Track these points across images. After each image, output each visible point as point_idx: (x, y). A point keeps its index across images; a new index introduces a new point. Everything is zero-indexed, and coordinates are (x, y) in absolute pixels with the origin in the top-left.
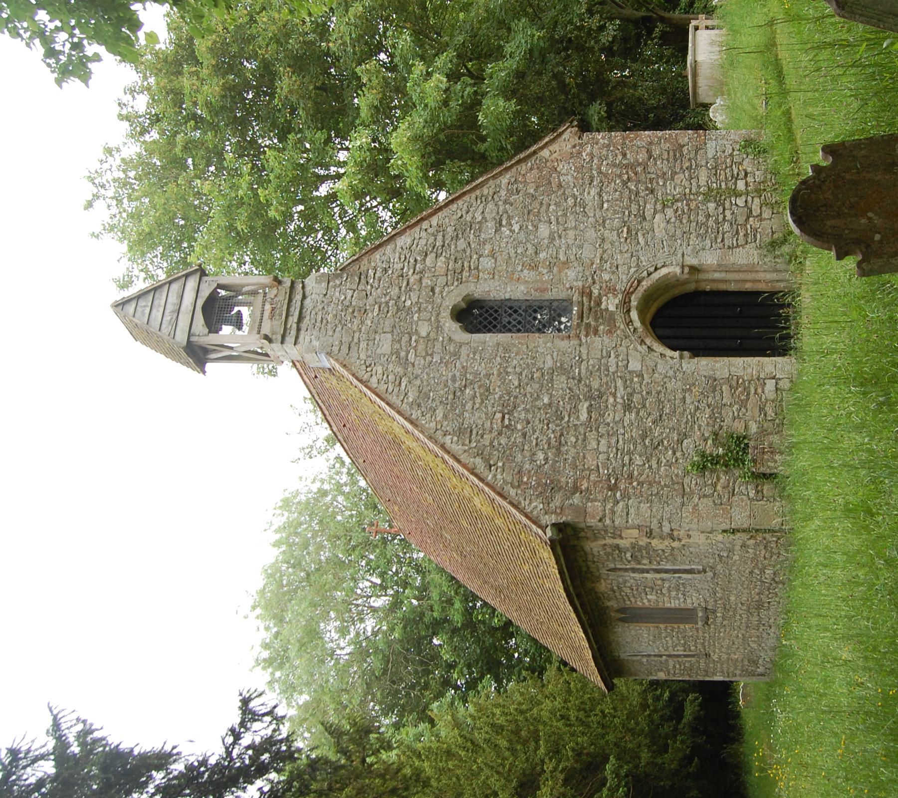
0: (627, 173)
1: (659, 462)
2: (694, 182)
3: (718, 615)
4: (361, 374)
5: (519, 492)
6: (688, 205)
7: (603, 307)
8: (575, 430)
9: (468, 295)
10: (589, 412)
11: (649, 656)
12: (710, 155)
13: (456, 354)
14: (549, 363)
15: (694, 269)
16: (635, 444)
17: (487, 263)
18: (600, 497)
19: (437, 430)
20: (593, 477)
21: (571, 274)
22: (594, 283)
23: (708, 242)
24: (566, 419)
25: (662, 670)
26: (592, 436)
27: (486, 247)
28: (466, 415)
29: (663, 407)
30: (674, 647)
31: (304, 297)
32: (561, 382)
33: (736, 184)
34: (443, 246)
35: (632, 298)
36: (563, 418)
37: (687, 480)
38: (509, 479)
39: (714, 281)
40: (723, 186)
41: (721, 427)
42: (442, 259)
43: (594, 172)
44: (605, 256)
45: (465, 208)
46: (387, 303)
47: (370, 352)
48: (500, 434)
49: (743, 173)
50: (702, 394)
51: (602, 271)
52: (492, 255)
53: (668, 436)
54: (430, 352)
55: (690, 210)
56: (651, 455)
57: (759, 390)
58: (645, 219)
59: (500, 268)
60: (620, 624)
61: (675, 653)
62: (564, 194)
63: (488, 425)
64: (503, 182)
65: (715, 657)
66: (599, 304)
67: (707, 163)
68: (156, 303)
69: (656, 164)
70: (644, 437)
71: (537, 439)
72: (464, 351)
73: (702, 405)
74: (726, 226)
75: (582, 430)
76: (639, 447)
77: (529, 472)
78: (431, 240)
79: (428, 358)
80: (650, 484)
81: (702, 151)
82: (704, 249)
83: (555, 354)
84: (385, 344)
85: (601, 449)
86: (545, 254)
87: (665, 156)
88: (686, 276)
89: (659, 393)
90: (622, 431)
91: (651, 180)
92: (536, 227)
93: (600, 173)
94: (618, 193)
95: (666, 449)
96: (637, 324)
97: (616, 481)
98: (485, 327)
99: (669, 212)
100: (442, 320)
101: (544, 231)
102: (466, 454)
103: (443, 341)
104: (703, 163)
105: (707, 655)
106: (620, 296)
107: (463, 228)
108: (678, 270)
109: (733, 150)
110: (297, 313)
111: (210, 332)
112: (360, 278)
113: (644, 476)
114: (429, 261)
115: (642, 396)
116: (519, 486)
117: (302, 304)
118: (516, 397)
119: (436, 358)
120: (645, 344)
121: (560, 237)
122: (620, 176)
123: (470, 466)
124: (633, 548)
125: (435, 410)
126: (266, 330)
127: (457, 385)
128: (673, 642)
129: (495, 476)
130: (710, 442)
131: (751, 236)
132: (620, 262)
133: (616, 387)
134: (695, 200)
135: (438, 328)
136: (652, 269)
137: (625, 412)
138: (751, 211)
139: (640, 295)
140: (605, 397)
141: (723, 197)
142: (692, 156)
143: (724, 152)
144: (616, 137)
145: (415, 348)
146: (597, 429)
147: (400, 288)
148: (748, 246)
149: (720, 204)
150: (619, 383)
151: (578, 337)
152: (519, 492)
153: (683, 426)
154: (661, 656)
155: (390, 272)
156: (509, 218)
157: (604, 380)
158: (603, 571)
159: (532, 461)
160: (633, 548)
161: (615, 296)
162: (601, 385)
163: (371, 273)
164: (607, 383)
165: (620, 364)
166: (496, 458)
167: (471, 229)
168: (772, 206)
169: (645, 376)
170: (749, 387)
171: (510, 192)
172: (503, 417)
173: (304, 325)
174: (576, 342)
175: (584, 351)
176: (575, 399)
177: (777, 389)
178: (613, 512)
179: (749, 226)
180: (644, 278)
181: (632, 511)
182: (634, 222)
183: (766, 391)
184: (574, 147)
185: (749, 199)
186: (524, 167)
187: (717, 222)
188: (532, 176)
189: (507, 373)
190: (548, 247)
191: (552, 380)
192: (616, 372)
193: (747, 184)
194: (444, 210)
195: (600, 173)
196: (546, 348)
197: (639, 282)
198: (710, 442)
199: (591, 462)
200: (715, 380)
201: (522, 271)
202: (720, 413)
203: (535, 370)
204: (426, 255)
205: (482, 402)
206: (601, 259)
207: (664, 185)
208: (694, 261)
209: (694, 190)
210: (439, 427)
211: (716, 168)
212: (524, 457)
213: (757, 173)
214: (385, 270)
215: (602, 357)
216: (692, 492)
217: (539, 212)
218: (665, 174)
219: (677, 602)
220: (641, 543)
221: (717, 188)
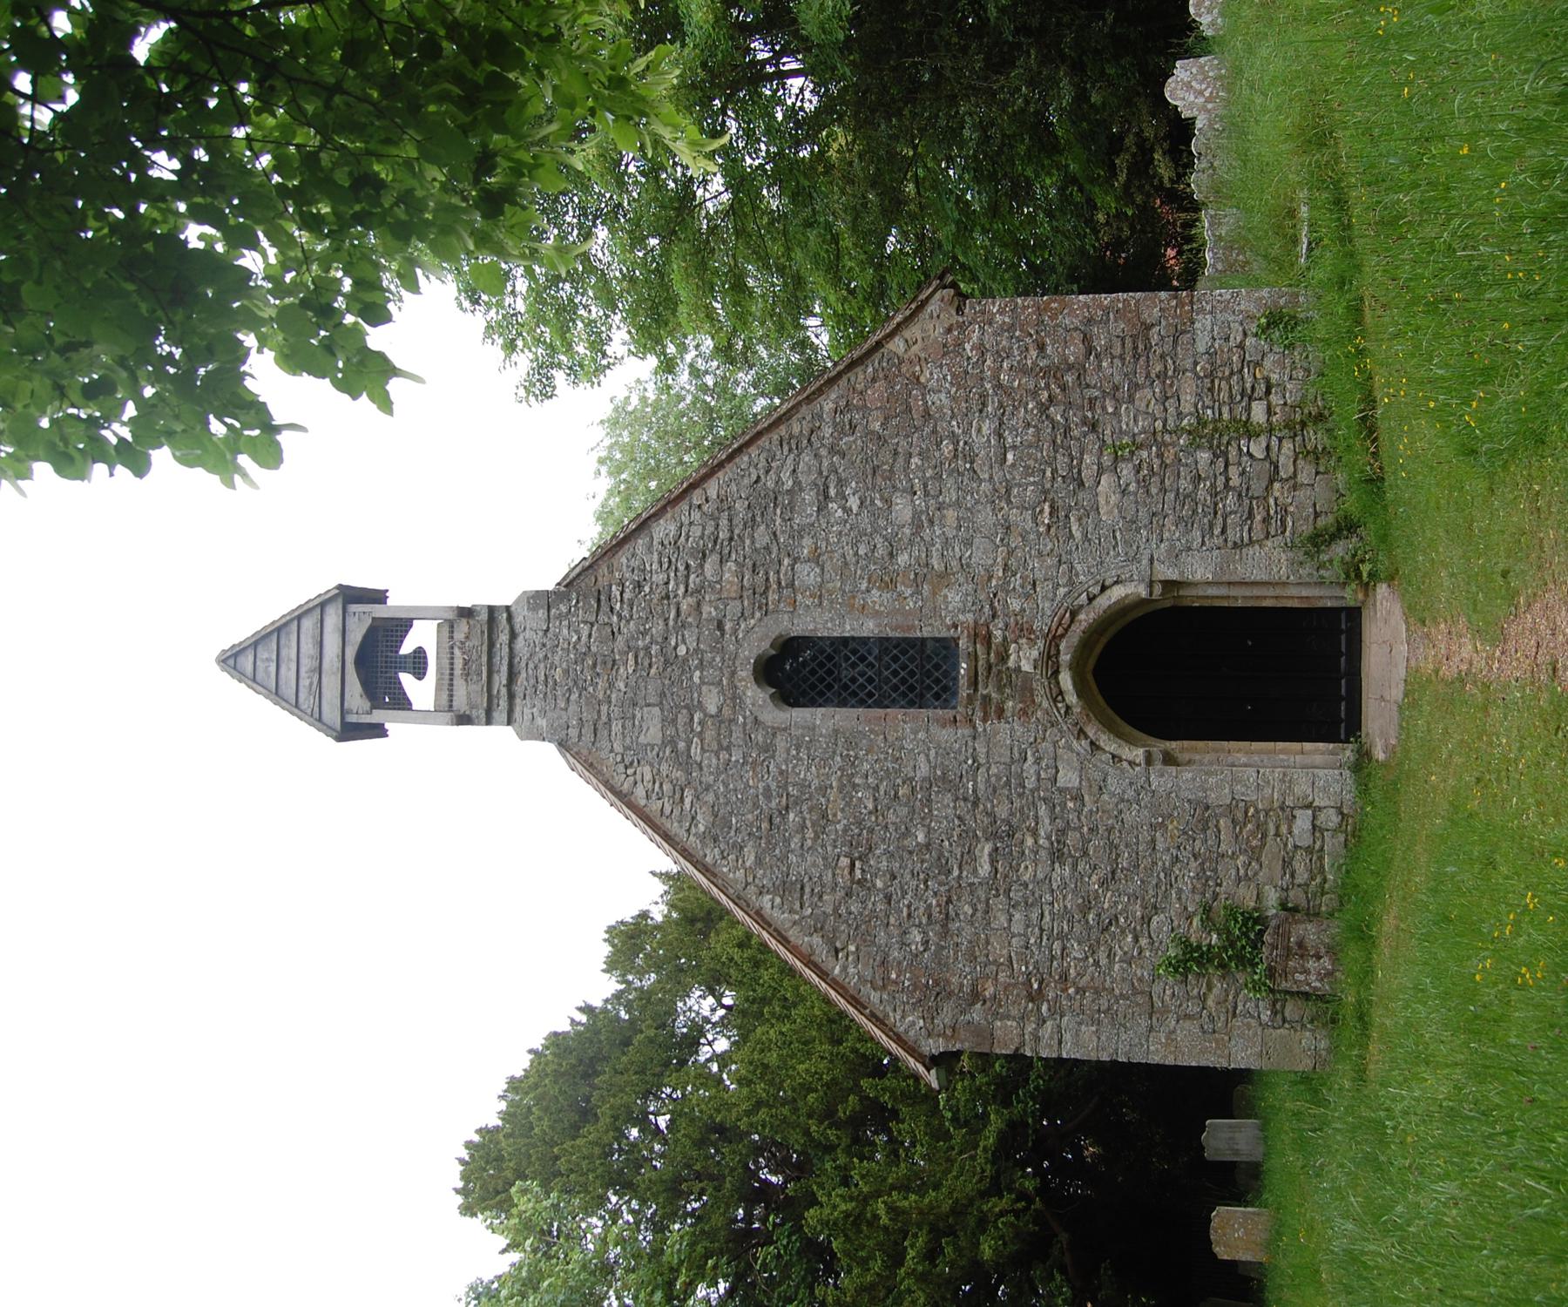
0: (1048, 386)
2: (1171, 405)
6: (1160, 455)
7: (1011, 663)
8: (972, 894)
13: (768, 749)
14: (924, 770)
15: (1168, 585)
17: (807, 575)
18: (1014, 1012)
19: (747, 884)
20: (1002, 977)
21: (954, 597)
22: (994, 616)
24: (956, 873)
26: (999, 904)
28: (793, 858)
29: (1118, 855)
31: (513, 635)
32: (944, 805)
33: (1248, 409)
34: (731, 539)
35: (1062, 646)
37: (1157, 989)
38: (868, 974)
40: (1226, 416)
41: (1216, 896)
43: (988, 386)
45: (763, 463)
46: (647, 649)
47: (628, 740)
48: (849, 895)
50: (1185, 833)
51: (1008, 592)
52: (815, 558)
53: (1125, 910)
54: (725, 744)
57: (1284, 829)
58: (1081, 484)
59: (830, 585)
62: (934, 432)
63: (828, 877)
64: (826, 408)
66: (1003, 658)
67: (1196, 363)
68: (284, 652)
69: (1100, 366)
70: (1085, 908)
71: (909, 907)
72: (781, 743)
74: (1231, 499)
75: (981, 893)
76: (1077, 928)
77: (899, 963)
78: (709, 529)
79: (724, 755)
80: (1097, 992)
81: (1185, 338)
82: (1189, 549)
83: (932, 752)
84: (652, 732)
85: (1015, 929)
86: (906, 557)
87: (1117, 351)
90: (1048, 897)
92: (888, 502)
93: (999, 386)
94: (1031, 430)
95: (1123, 932)
96: (1072, 698)
97: (1040, 984)
99: (1126, 470)
101: (903, 509)
102: (797, 928)
103: (745, 724)
104: (1188, 364)
106: (1040, 643)
109: (1245, 334)
110: (505, 668)
111: (374, 707)
112: (599, 601)
113: (1087, 978)
114: (709, 567)
115: (1082, 835)
117: (511, 649)
119: (736, 756)
120: (1086, 737)
121: (931, 522)
122: (1034, 394)
123: (805, 949)
125: (742, 848)
126: (460, 703)
127: (773, 805)
129: (844, 969)
130: (1196, 921)
131: (1276, 522)
132: (1039, 575)
133: (1036, 817)
134: (1173, 444)
135: (736, 699)
136: (1096, 590)
138: (1276, 467)
141: (1225, 439)
142: (1167, 348)
143: (1227, 339)
144: (1025, 308)
145: (700, 735)
147: (666, 620)
148: (1269, 543)
149: (1219, 453)
150: (1043, 810)
155: (647, 589)
156: (841, 483)
157: (1017, 804)
159: (903, 944)
162: (1012, 814)
163: (615, 590)
164: (1021, 810)
165: (1043, 775)
166: (844, 936)
167: (776, 506)
168: (1315, 455)
169: (1086, 798)
170: (1266, 823)
171: (840, 431)
172: (853, 865)
173: (518, 689)
174: (967, 731)
175: (982, 750)
176: (969, 838)
177: (1314, 826)
178: (1037, 1039)
179: (1272, 501)
181: (1067, 1037)
182: (1062, 491)
183: (1296, 831)
184: (949, 330)
185: (1274, 442)
188: (876, 393)
189: (854, 786)
191: (929, 800)
192: (1038, 789)
193: (1270, 411)
194: (728, 467)
195: (999, 386)
196: (916, 737)
197: (1074, 614)
198: (1196, 921)
199: (998, 950)
200: (1207, 808)
202: (1215, 870)
203: (899, 781)
204: (704, 555)
205: (817, 837)
206: (1006, 568)
207: (1116, 413)
208: (1172, 575)
209: (1171, 424)
210: (750, 879)
211: (1211, 375)
212: (890, 936)
214: (639, 586)
215: (1013, 761)
216: (1166, 1010)
217: (891, 471)
218: (1116, 388)
221: (1215, 421)
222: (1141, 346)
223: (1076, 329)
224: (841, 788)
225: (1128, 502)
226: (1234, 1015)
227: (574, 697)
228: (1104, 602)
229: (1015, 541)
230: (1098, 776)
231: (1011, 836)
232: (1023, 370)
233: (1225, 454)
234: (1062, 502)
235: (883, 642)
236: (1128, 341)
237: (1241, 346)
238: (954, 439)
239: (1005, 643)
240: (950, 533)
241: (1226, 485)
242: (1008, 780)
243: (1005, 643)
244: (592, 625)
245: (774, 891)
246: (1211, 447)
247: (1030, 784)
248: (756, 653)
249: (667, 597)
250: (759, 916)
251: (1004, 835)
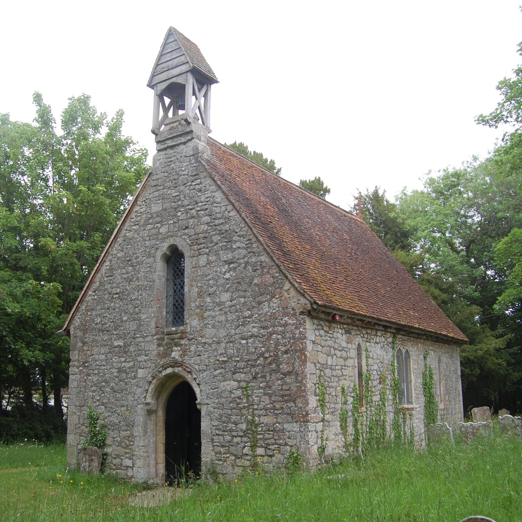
0: (270, 356)
1: (94, 391)
2: (263, 412)
4: (141, 199)
5: (84, 311)
6: (244, 407)
7: (175, 348)
10: (119, 346)
12: (286, 426)
13: (149, 256)
14: (143, 317)
16: (102, 376)
17: (203, 260)
19: (112, 255)
23: (216, 423)
24: (115, 333)
27: (214, 257)
31: (184, 143)
32: (132, 326)
33: (261, 447)
34: (215, 226)
35: (180, 368)
36: (115, 330)
37: (86, 408)
38: (89, 304)
40: (259, 436)
43: (271, 329)
44: (207, 346)
45: (242, 233)
48: (110, 294)
49: (271, 453)
51: (197, 345)
52: (209, 263)
53: (105, 396)
55: (241, 409)
56: (97, 387)
57: (127, 455)
59: (199, 271)
62: (254, 307)
66: (176, 345)
67: (279, 423)
68: (174, 52)
69: (278, 380)
70: (106, 381)
71: (106, 316)
72: (151, 260)
73: (120, 418)
74: (228, 438)
78: (218, 216)
79: (147, 238)
81: (290, 419)
82: (211, 420)
83: (148, 320)
87: (285, 387)
89: (126, 390)
91: (264, 377)
92: (227, 291)
93: (271, 334)
94: (253, 350)
96: (164, 373)
97: (87, 366)
99: (239, 393)
100: (168, 240)
101: (225, 297)
103: (156, 244)
104: (279, 420)
106: (180, 359)
107: (228, 237)
109: (291, 446)
110: (173, 144)
114: (207, 219)
115: (125, 379)
118: (126, 299)
121: (221, 310)
122: (268, 351)
123: (95, 280)
125: (122, 251)
129: (90, 295)
134: (248, 413)
135: (163, 240)
137: (117, 369)
139: (182, 374)
142: (286, 410)
143: (289, 438)
146: (110, 352)
147: (189, 205)
148: (213, 454)
150: (131, 364)
152: (84, 311)
153: (110, 405)
155: (199, 194)
157: (133, 354)
161: (181, 356)
162: (131, 352)
164: (132, 356)
165: (141, 363)
167: (227, 242)
169: (135, 380)
171: (254, 265)
172: (117, 294)
175: (148, 339)
178: (73, 366)
179: (228, 455)
180: (192, 375)
183: (127, 460)
184: (293, 309)
186: (274, 271)
187: (231, 431)
188: (268, 279)
189: (138, 291)
190: (214, 302)
191: (135, 320)
192: (137, 362)
197: (190, 372)
199: (96, 350)
200: (133, 426)
201: (197, 287)
204: (210, 215)
205: (125, 279)
207: (260, 388)
209: (256, 412)
210: (113, 256)
211: (274, 430)
213: (271, 465)
214: (200, 191)
215: (145, 351)
217: (239, 290)
221: (257, 432)
222: (286, 398)
223: (294, 368)
224: (138, 286)
225: (227, 394)
226: (80, 436)
227: (166, 174)
229: (214, 346)
230: (141, 384)
231: (125, 352)
232: (277, 344)
233: (245, 436)
234: (226, 366)
235: (183, 295)
236: (289, 392)
237: (286, 444)
238: (250, 316)
239: (180, 345)
240: (216, 318)
241: (233, 436)
243: (180, 345)
244: (188, 175)
245: (111, 266)
246: (248, 430)
247: (139, 359)
248: (178, 244)
249: (197, 203)
250: (103, 261)
251: (124, 350)
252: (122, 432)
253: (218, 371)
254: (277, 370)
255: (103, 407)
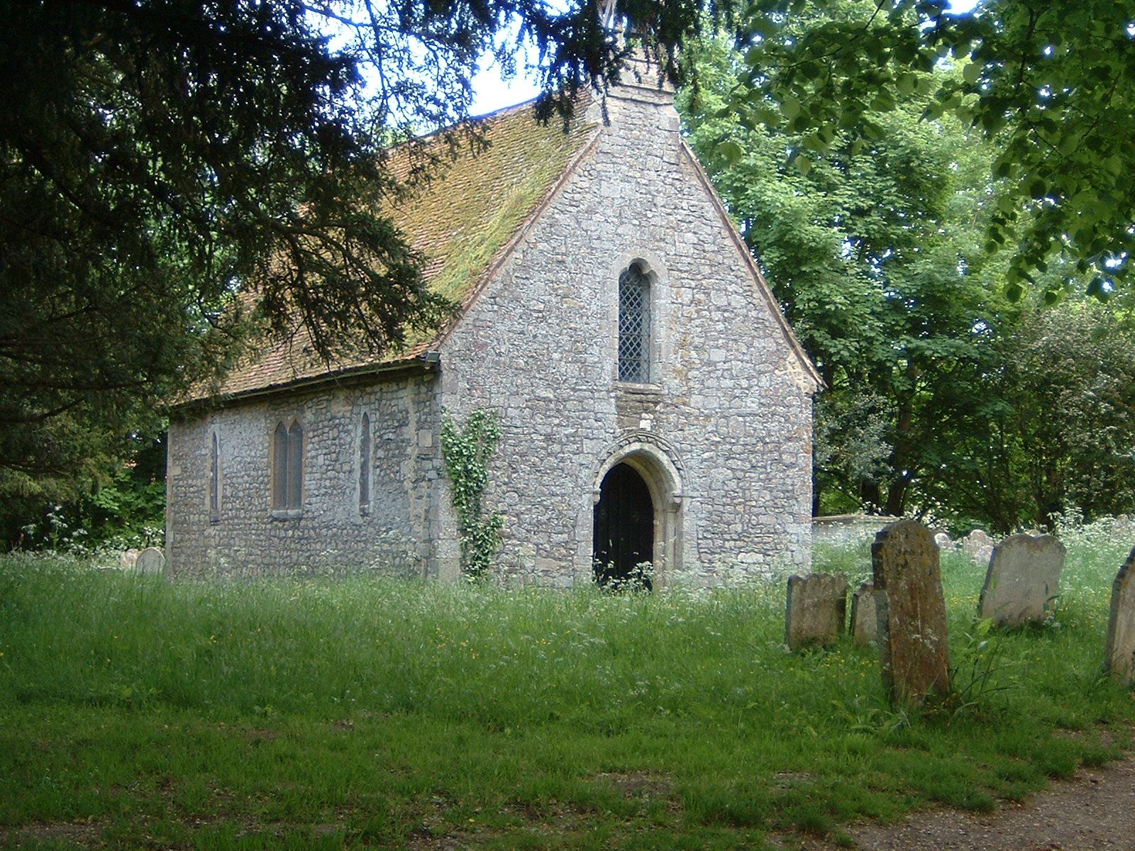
3: (290, 532)
6: (740, 504)
7: (644, 415)
9: (657, 276)
11: (214, 456)
15: (677, 507)
25: (184, 470)
30: (232, 485)
31: (656, 105)
39: (665, 528)
42: (692, 251)
45: (739, 274)
57: (563, 571)
60: (274, 426)
61: (220, 487)
65: (211, 531)
66: (646, 410)
74: (719, 542)
76: (510, 449)
88: (671, 501)
91: (765, 467)
96: (627, 450)
98: (624, 294)
99: (733, 484)
105: (215, 522)
108: (678, 492)
116: (475, 326)
117: (650, 103)
124: (403, 441)
128: (239, 484)
129: (485, 303)
140: (558, 415)
151: (617, 389)
154: (214, 469)
158: (364, 409)
160: (403, 441)
170: (566, 560)
172: (540, 312)
186: (779, 335)
191: (576, 362)
194: (738, 253)
200: (573, 527)
208: (685, 509)
219: (312, 487)
220: (409, 450)
228: (673, 470)
231: (558, 411)
242: (586, 410)
243: (653, 412)
249: (676, 208)
252: (554, 536)
253: (706, 455)
254: (779, 461)
255: (516, 495)
